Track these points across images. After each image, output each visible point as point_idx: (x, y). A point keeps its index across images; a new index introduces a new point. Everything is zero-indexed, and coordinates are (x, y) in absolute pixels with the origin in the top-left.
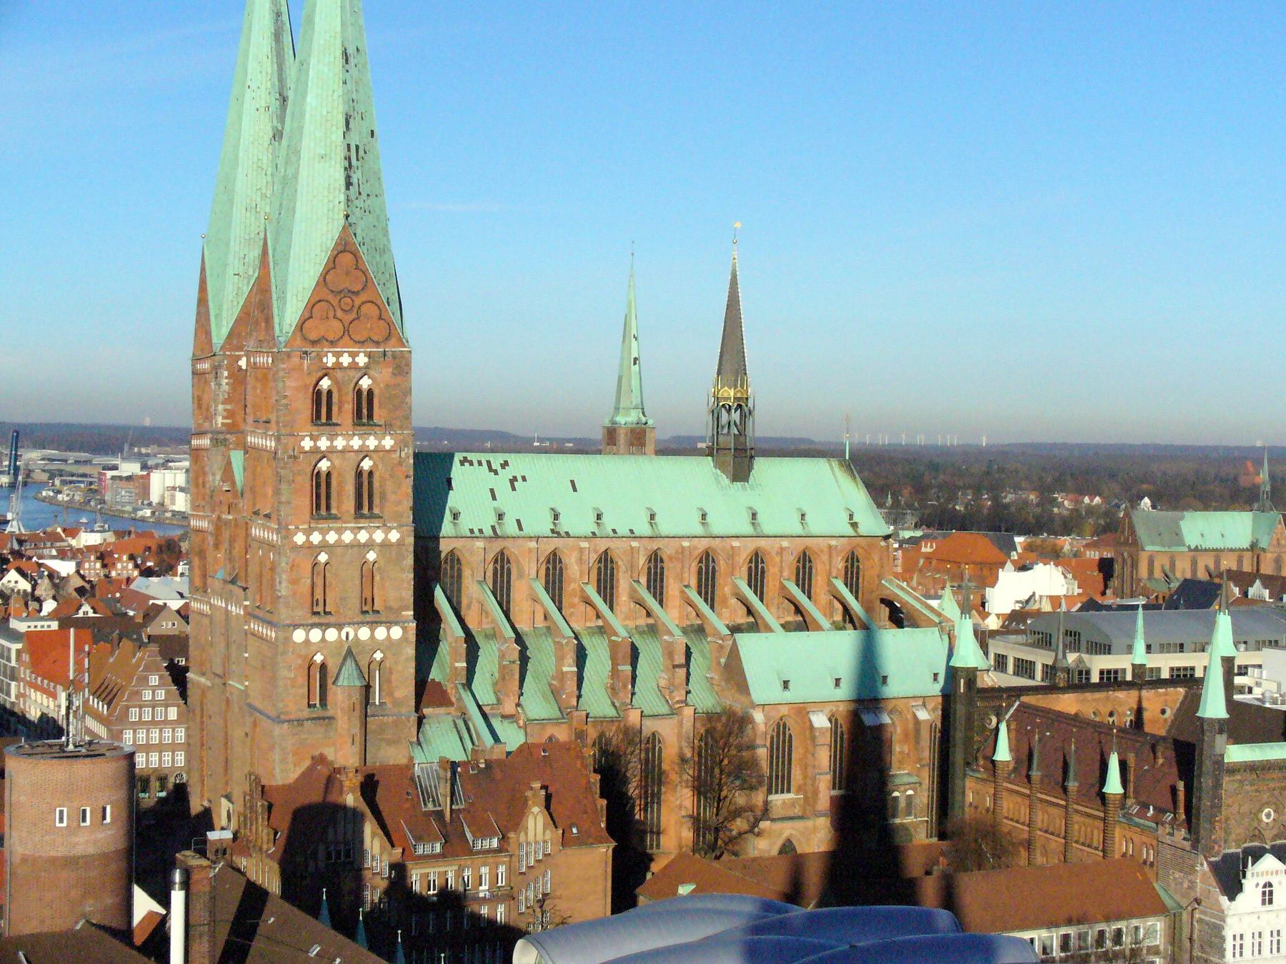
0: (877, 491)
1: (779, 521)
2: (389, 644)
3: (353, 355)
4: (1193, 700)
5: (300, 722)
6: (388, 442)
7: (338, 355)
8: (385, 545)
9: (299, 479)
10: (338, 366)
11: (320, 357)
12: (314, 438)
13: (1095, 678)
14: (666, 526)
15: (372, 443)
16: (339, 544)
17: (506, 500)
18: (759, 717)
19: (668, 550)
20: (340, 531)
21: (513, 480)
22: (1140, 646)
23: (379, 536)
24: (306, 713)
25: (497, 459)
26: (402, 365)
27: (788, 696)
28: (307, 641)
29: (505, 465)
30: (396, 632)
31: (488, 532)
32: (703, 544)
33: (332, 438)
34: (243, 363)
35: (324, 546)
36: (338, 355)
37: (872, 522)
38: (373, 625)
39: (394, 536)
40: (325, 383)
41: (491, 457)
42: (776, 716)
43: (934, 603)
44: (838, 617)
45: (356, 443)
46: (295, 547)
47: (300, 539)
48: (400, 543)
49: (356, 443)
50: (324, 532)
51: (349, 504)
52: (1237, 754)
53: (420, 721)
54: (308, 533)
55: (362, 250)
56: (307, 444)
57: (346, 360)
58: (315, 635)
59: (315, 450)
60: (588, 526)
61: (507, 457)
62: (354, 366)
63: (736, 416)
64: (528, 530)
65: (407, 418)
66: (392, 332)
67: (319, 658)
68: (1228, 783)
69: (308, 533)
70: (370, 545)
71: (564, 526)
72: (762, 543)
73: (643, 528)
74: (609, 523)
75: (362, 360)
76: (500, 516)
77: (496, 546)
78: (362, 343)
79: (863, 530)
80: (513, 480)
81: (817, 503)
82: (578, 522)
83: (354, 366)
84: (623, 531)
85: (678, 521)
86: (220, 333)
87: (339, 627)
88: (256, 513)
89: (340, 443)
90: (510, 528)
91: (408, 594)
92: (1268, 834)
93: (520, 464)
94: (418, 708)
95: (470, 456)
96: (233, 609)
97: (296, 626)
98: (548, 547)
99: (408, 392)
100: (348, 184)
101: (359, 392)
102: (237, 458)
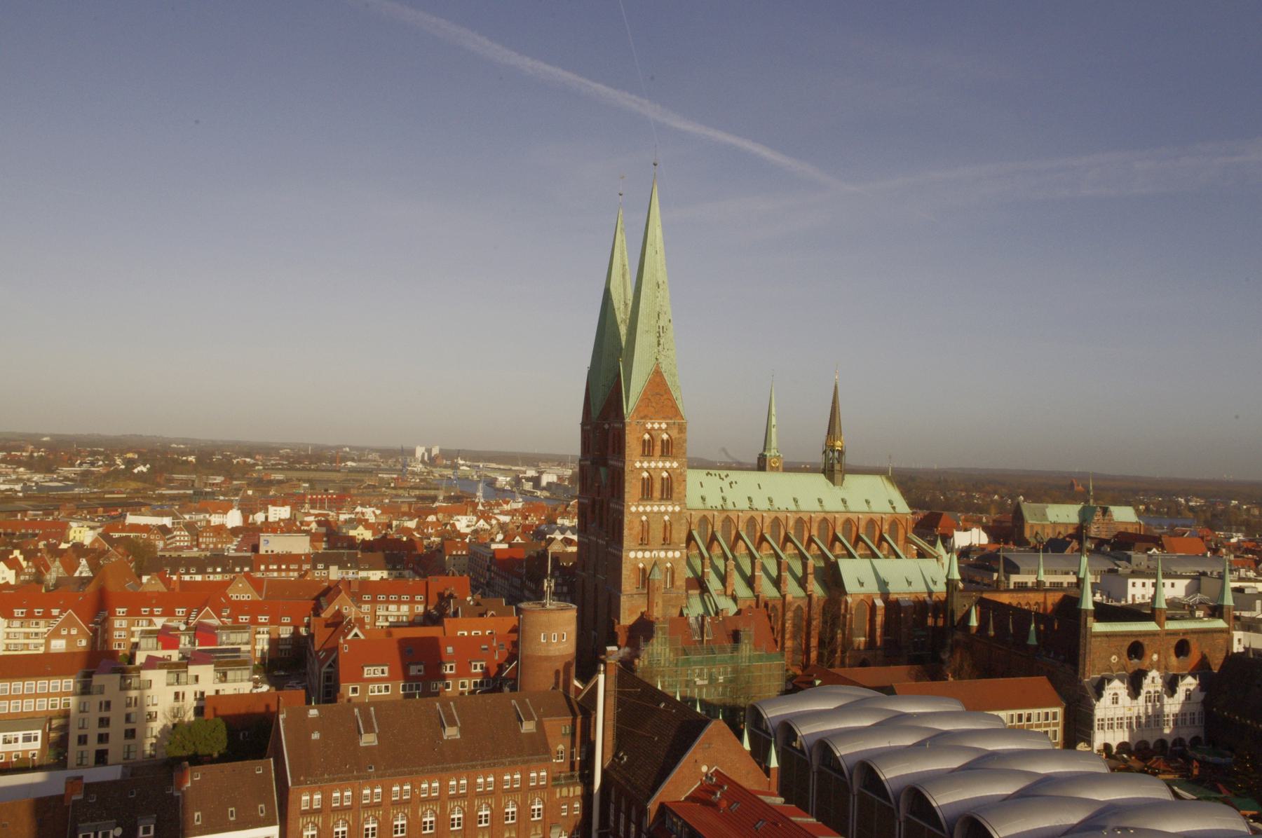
0: (906, 493)
1: (856, 505)
2: (673, 561)
5: (632, 595)
6: (675, 465)
8: (673, 513)
10: (653, 429)
11: (644, 424)
13: (1012, 587)
14: (804, 506)
15: (668, 465)
16: (652, 512)
17: (728, 493)
18: (849, 600)
19: (806, 518)
20: (652, 506)
22: (1042, 571)
24: (635, 591)
25: (723, 473)
26: (682, 429)
27: (863, 590)
30: (677, 554)
32: (823, 515)
34: (606, 426)
35: (645, 513)
37: (902, 507)
38: (667, 550)
39: (677, 509)
40: (647, 437)
45: (660, 465)
46: (631, 513)
47: (633, 509)
48: (680, 512)
49: (660, 465)
50: (645, 506)
52: (1098, 627)
53: (687, 598)
54: (637, 506)
56: (638, 465)
57: (656, 426)
58: (640, 554)
59: (642, 468)
60: (766, 506)
61: (729, 472)
62: (660, 429)
63: (836, 454)
66: (676, 412)
67: (641, 566)
68: (1095, 644)
69: (637, 506)
70: (666, 512)
71: (755, 505)
72: (849, 515)
73: (792, 507)
74: (777, 504)
76: (724, 499)
77: (724, 515)
78: (664, 418)
79: (898, 510)
83: (660, 429)
84: (783, 508)
85: (808, 505)
86: (595, 413)
87: (651, 551)
89: (653, 465)
90: (730, 506)
91: (684, 536)
92: (1114, 668)
93: (734, 475)
95: (712, 472)
96: (600, 541)
99: (685, 441)
102: (603, 470)
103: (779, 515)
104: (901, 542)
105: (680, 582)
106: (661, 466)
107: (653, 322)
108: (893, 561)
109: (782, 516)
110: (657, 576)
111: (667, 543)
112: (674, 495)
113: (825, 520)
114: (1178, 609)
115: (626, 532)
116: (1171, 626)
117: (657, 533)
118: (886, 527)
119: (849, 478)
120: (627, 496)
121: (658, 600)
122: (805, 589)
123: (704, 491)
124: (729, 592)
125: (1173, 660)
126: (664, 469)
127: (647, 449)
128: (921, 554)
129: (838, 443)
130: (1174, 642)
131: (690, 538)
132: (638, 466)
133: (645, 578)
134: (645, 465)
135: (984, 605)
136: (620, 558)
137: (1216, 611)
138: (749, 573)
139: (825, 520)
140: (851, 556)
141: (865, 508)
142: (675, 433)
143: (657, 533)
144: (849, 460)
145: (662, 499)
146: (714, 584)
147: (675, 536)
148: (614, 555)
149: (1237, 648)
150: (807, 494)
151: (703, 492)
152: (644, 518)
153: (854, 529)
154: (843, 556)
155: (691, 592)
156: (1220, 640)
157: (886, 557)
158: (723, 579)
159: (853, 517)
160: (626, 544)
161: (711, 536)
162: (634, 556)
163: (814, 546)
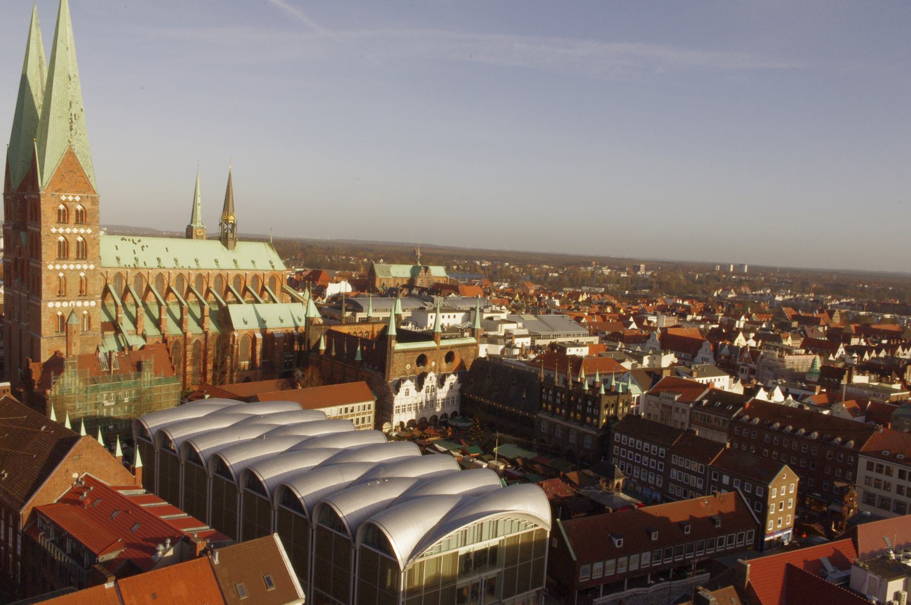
0: (282, 255)
1: (245, 265)
2: (89, 309)
3: (74, 196)
4: (386, 329)
5: (52, 338)
6: (89, 231)
7: (67, 196)
8: (88, 270)
9: (50, 244)
10: (67, 200)
11: (59, 196)
12: (57, 228)
14: (203, 265)
15: (82, 231)
16: (68, 269)
18: (236, 334)
19: (205, 274)
20: (68, 264)
21: (143, 247)
22: (371, 310)
23: (85, 267)
24: (54, 334)
25: (136, 239)
26: (95, 201)
27: (246, 327)
28: (54, 307)
29: (139, 241)
30: (93, 303)
31: (132, 266)
32: (218, 272)
33: (64, 228)
35: (62, 270)
36: (67, 196)
37: (280, 265)
39: (92, 267)
40: (62, 207)
41: (133, 238)
42: (243, 334)
43: (301, 294)
44: (266, 299)
45: (75, 231)
46: (49, 270)
47: (51, 267)
48: (95, 270)
49: (75, 231)
50: (61, 265)
51: (73, 254)
53: (103, 337)
54: (54, 265)
55: (78, 156)
56: (54, 230)
57: (70, 198)
58: (58, 304)
59: (57, 234)
60: (173, 265)
62: (74, 201)
63: (230, 226)
64: (148, 266)
65: (98, 222)
67: (60, 313)
69: (54, 265)
70: (82, 270)
71: (163, 264)
72: (239, 272)
73: (194, 266)
74: (181, 264)
75: (78, 199)
77: (136, 272)
78: (77, 192)
79: (276, 268)
80: (143, 247)
81: (260, 259)
82: (168, 263)
83: (74, 201)
84: (186, 266)
85: (207, 264)
87: (68, 301)
88: (32, 256)
89: (68, 230)
90: (141, 265)
93: (145, 241)
94: (102, 333)
97: (49, 301)
98: (157, 272)
99: (98, 212)
100: (71, 129)
101: (77, 211)
103: (183, 272)
104: (278, 292)
105: (96, 326)
106: (75, 232)
107: (66, 109)
108: (271, 305)
109: (185, 273)
110: (74, 321)
111: (83, 294)
112: (89, 256)
113: (220, 275)
114: (454, 332)
115: (44, 286)
116: (444, 343)
117: (73, 286)
118: (267, 280)
119: (239, 244)
120: (44, 257)
121: (76, 340)
122: (202, 328)
123: (115, 253)
124: (140, 332)
125: (444, 365)
126: (78, 234)
127: (63, 217)
128: (294, 300)
129: (231, 218)
130: (445, 353)
131: (106, 290)
132: (53, 231)
133: (63, 324)
134: (61, 230)
135: (330, 334)
136: (39, 308)
137: (473, 333)
138: (157, 316)
139: (220, 275)
140: (239, 302)
141: (251, 267)
142: (88, 205)
143: (73, 286)
144: (239, 230)
145: (78, 259)
146: (126, 325)
147: (91, 289)
148: (33, 305)
149: (482, 354)
150: (206, 256)
151: (118, 253)
152: (61, 275)
153: (243, 282)
154: (234, 303)
155: (106, 333)
156: (472, 351)
157: (267, 302)
158: (135, 321)
159: (242, 273)
160: (44, 296)
161: (120, 291)
162: (52, 306)
163: (211, 295)
